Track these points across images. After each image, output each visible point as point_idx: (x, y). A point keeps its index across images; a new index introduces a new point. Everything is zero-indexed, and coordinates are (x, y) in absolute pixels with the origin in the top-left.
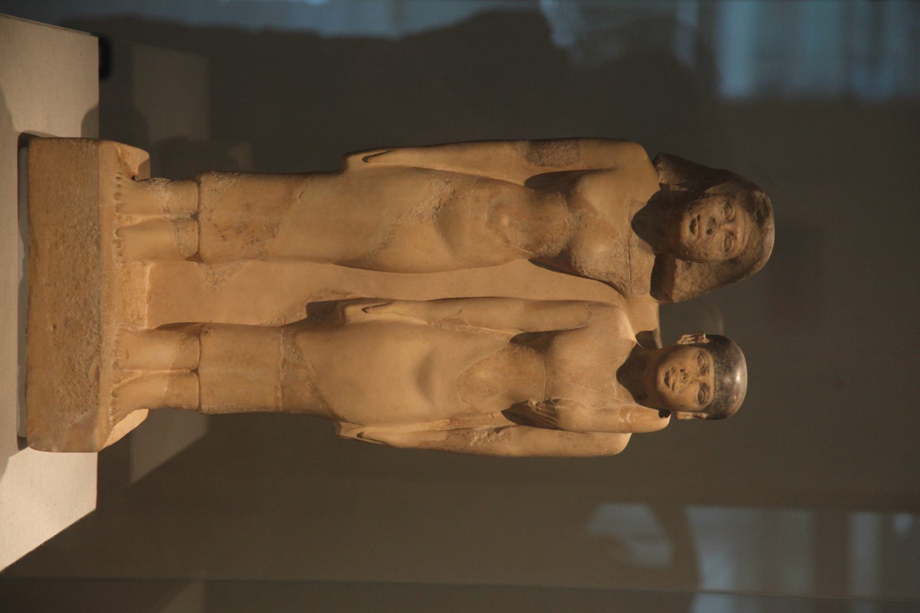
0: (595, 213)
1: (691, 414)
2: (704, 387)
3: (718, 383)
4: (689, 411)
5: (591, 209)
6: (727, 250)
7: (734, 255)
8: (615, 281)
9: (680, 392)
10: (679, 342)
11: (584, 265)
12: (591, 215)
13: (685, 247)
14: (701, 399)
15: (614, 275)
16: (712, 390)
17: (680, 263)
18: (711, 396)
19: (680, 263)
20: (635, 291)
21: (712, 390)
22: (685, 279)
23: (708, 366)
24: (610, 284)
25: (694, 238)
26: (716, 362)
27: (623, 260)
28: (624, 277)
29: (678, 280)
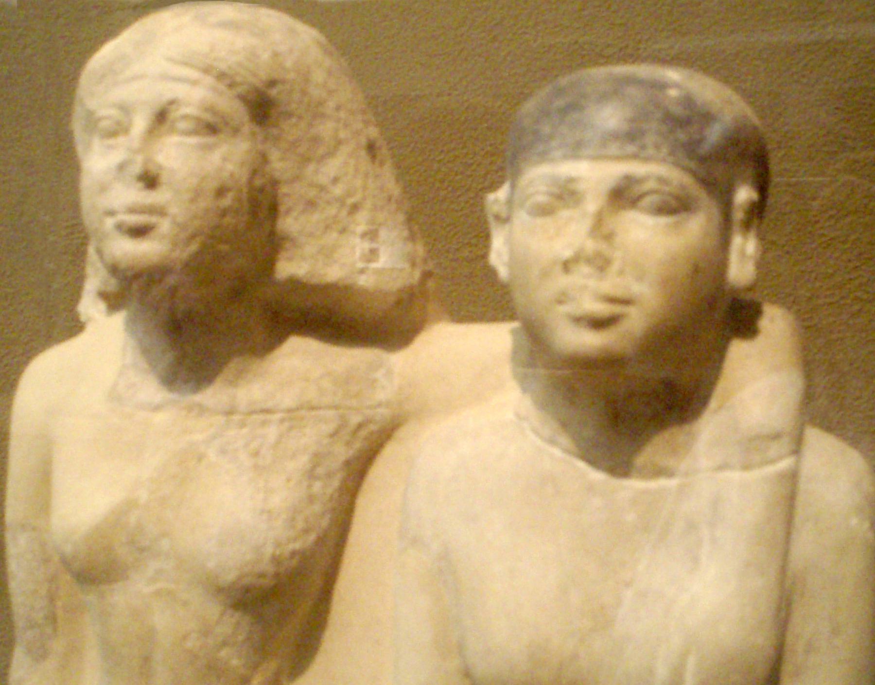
0: (130, 505)
1: (737, 240)
2: (623, 196)
3: (614, 149)
4: (725, 243)
5: (117, 518)
6: (212, 129)
7: (237, 111)
8: (342, 452)
9: (640, 279)
10: (503, 272)
11: (269, 550)
12: (133, 519)
13: (200, 252)
14: (676, 206)
15: (318, 458)
16: (637, 169)
17: (288, 268)
18: (657, 171)
19: (288, 268)
20: (381, 395)
21: (637, 169)
22: (328, 253)
23: (555, 181)
24: (358, 470)
25: (165, 226)
26: (544, 157)
27: (272, 433)
28: (330, 427)
29: (333, 274)
